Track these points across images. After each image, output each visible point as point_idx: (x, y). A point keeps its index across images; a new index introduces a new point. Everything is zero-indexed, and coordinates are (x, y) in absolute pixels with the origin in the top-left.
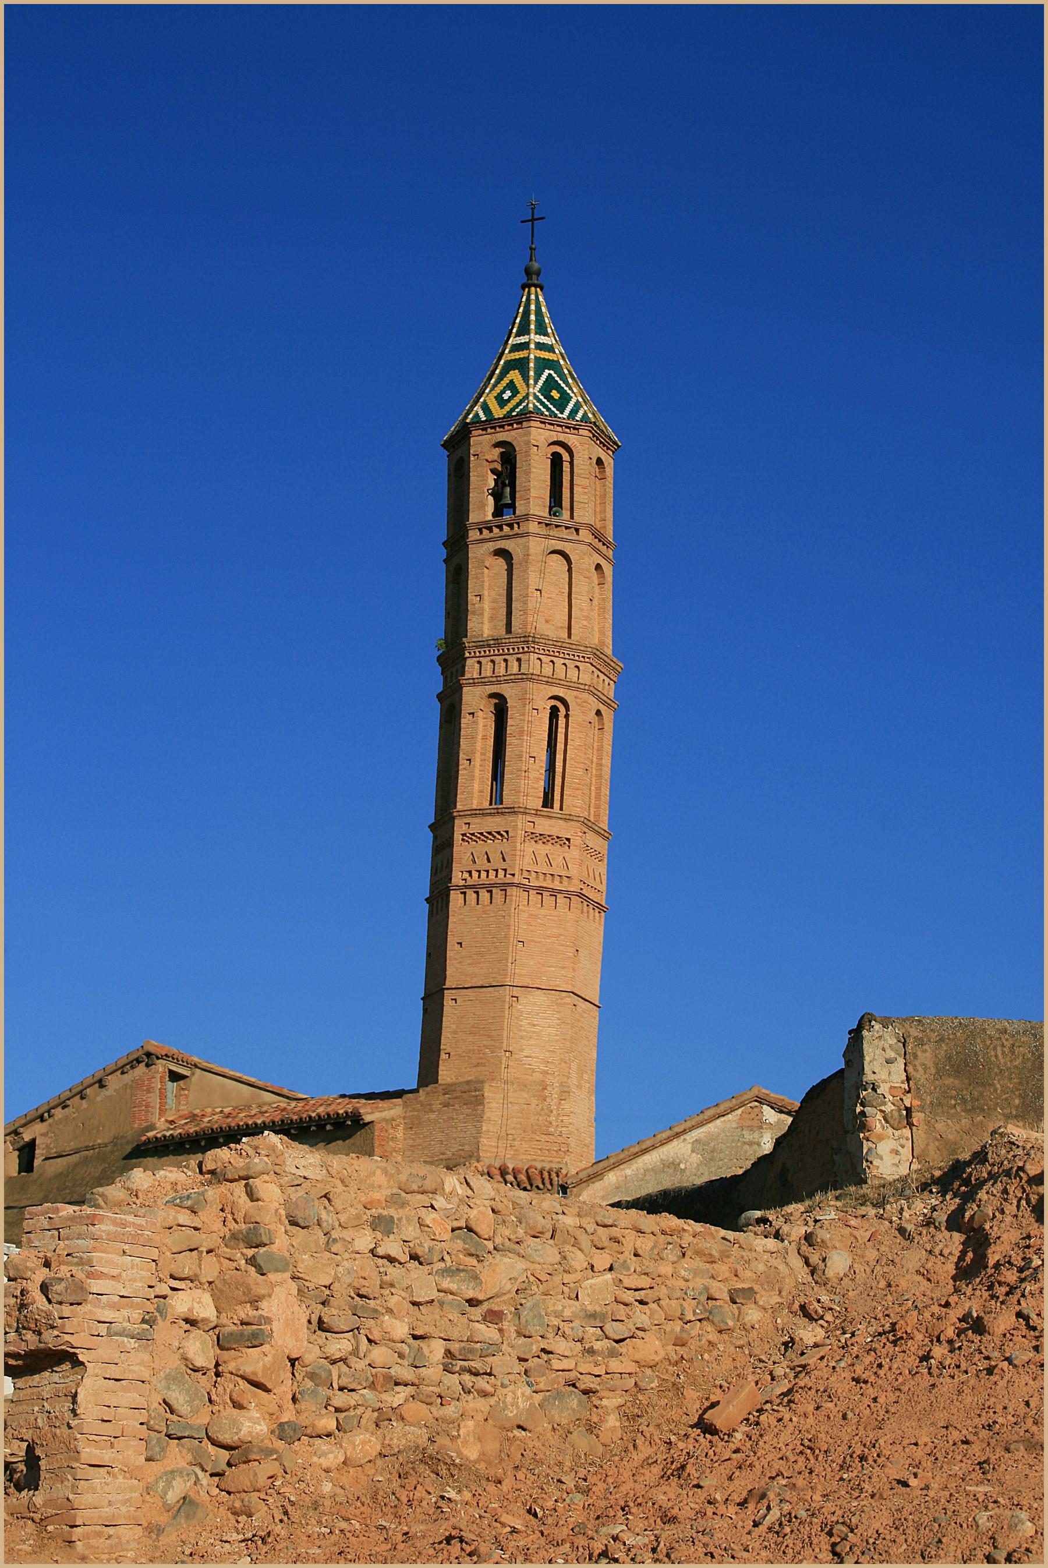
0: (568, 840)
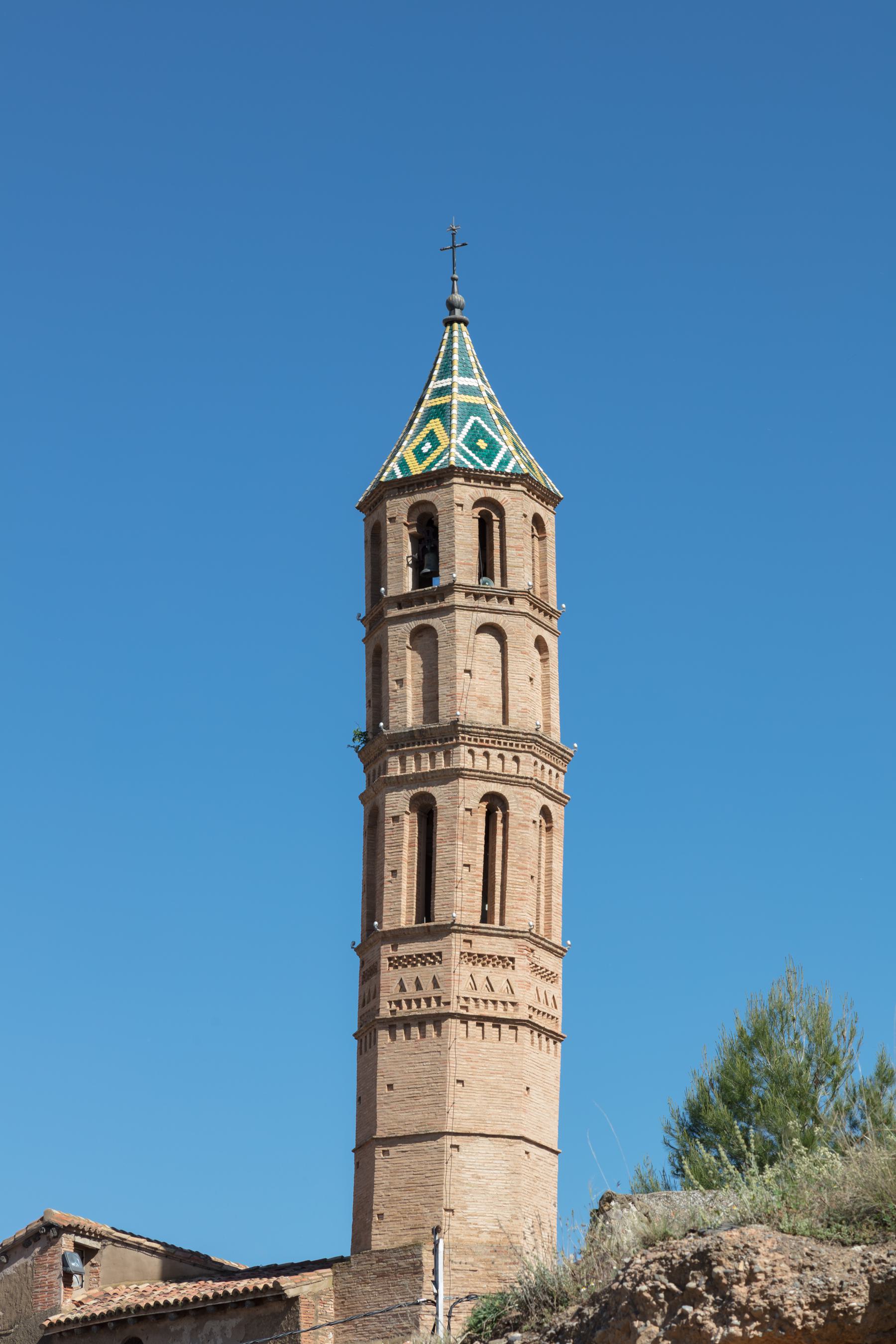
0: (512, 959)
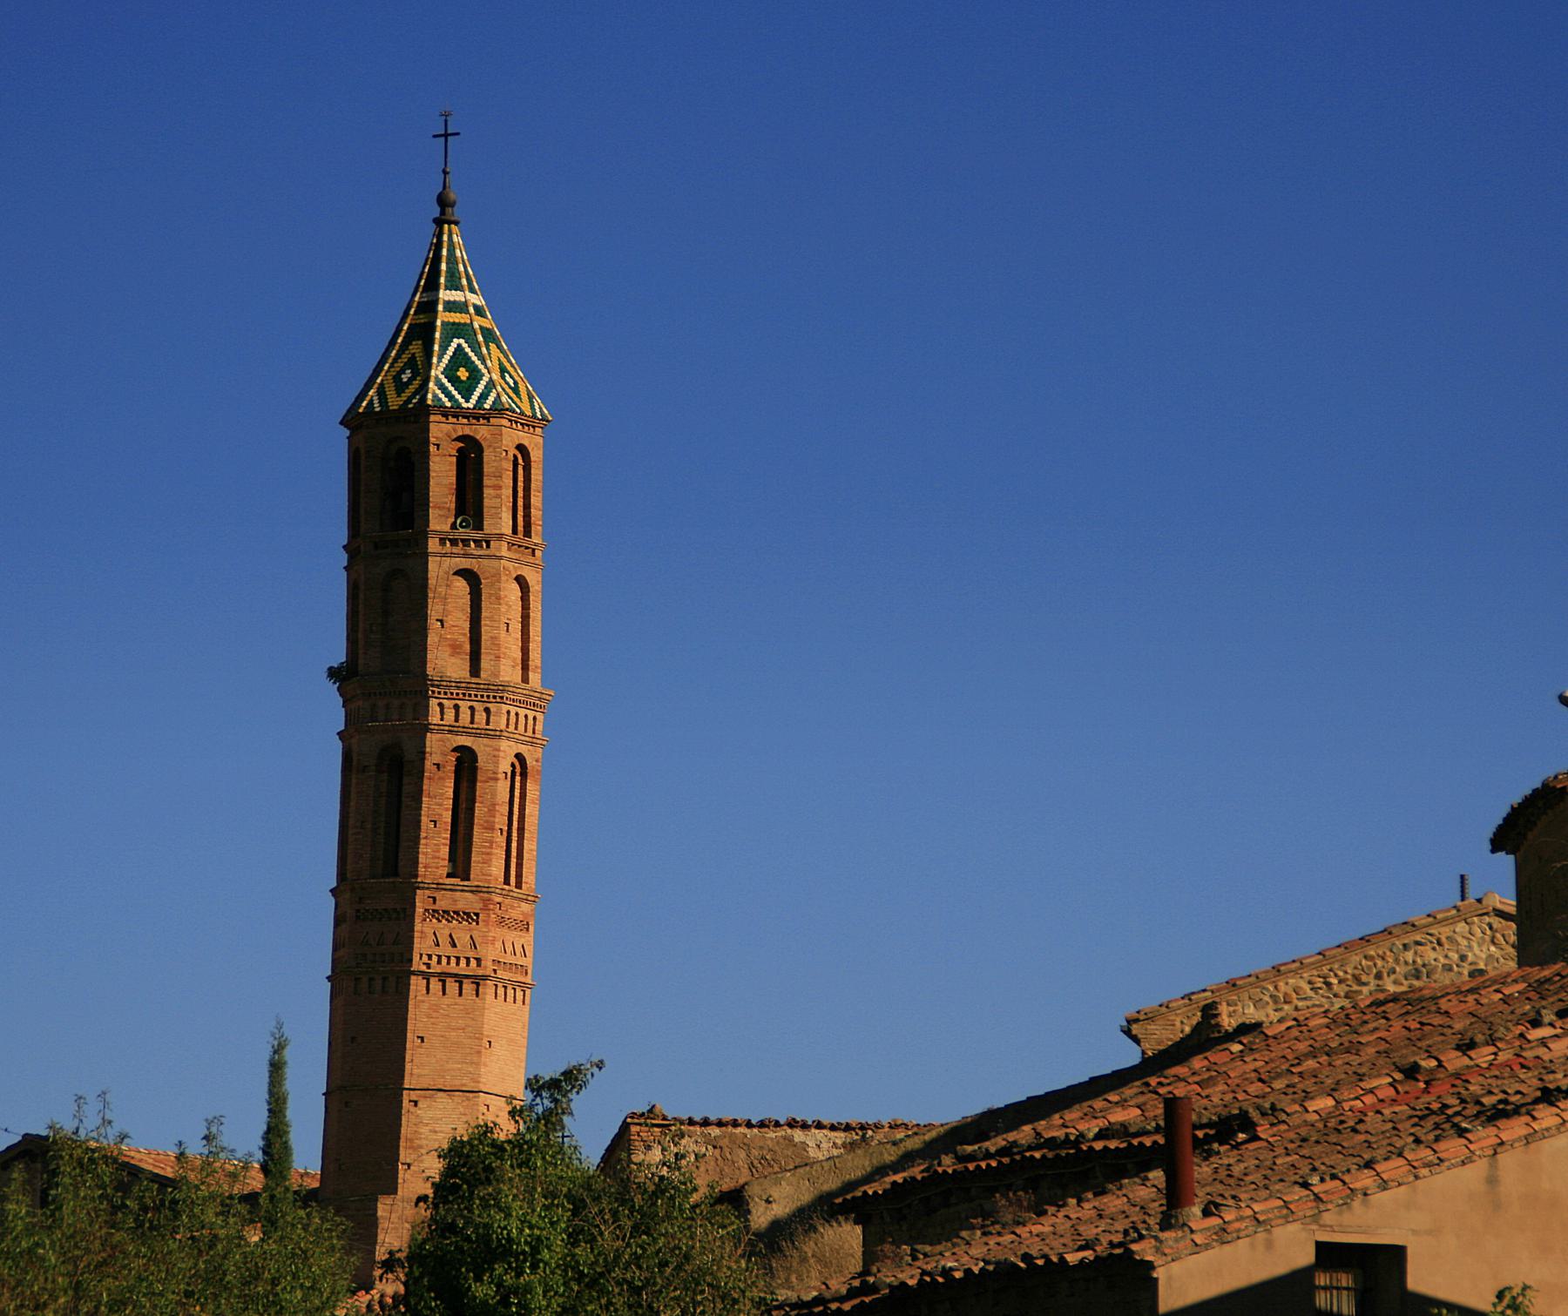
0: (477, 915)
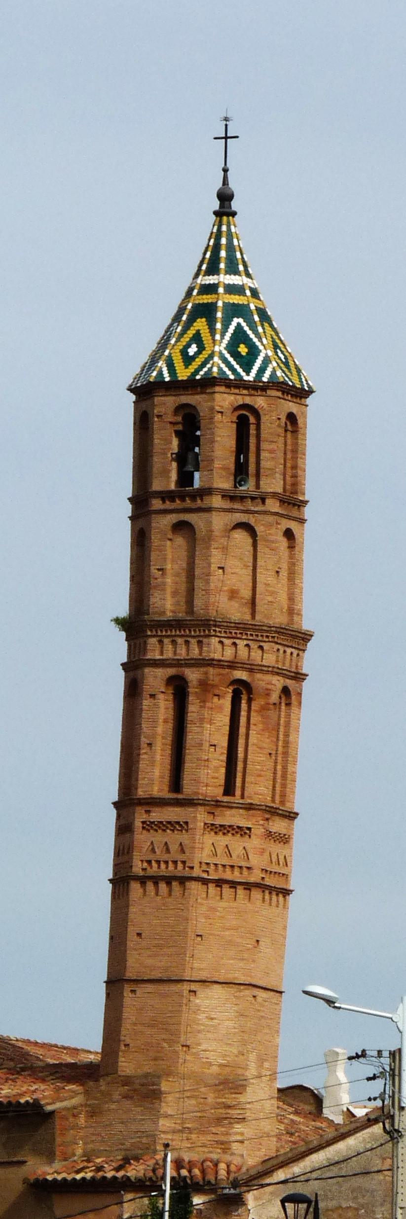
0: (249, 829)
